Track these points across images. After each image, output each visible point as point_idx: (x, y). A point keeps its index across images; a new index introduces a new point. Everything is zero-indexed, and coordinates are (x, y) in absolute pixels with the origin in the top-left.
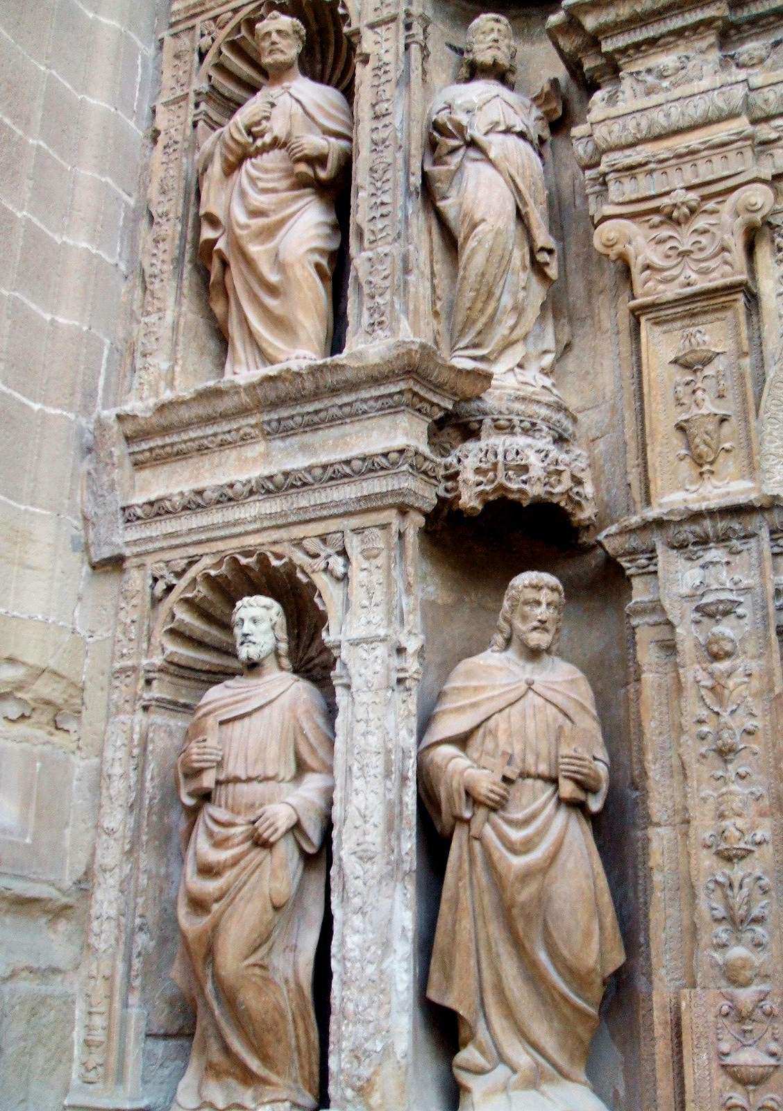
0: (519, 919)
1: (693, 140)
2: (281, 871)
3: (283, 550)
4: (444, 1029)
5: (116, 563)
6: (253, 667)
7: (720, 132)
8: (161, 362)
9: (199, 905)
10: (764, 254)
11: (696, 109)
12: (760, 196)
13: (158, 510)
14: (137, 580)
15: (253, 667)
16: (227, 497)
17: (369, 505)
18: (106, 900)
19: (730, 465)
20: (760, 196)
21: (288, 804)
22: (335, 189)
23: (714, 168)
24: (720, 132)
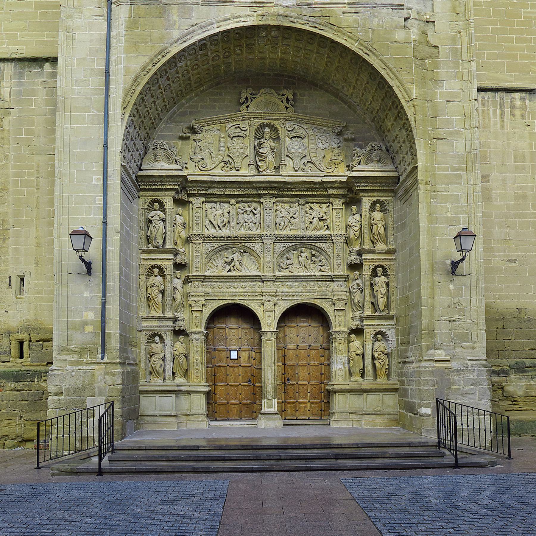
0: (180, 365)
2: (161, 362)
3: (159, 332)
4: (174, 373)
6: (157, 343)
8: (143, 309)
9: (154, 364)
12: (204, 302)
13: (146, 327)
14: (143, 333)
15: (157, 343)
16: (154, 327)
19: (199, 327)
20: (204, 302)
21: (162, 355)
22: (163, 292)
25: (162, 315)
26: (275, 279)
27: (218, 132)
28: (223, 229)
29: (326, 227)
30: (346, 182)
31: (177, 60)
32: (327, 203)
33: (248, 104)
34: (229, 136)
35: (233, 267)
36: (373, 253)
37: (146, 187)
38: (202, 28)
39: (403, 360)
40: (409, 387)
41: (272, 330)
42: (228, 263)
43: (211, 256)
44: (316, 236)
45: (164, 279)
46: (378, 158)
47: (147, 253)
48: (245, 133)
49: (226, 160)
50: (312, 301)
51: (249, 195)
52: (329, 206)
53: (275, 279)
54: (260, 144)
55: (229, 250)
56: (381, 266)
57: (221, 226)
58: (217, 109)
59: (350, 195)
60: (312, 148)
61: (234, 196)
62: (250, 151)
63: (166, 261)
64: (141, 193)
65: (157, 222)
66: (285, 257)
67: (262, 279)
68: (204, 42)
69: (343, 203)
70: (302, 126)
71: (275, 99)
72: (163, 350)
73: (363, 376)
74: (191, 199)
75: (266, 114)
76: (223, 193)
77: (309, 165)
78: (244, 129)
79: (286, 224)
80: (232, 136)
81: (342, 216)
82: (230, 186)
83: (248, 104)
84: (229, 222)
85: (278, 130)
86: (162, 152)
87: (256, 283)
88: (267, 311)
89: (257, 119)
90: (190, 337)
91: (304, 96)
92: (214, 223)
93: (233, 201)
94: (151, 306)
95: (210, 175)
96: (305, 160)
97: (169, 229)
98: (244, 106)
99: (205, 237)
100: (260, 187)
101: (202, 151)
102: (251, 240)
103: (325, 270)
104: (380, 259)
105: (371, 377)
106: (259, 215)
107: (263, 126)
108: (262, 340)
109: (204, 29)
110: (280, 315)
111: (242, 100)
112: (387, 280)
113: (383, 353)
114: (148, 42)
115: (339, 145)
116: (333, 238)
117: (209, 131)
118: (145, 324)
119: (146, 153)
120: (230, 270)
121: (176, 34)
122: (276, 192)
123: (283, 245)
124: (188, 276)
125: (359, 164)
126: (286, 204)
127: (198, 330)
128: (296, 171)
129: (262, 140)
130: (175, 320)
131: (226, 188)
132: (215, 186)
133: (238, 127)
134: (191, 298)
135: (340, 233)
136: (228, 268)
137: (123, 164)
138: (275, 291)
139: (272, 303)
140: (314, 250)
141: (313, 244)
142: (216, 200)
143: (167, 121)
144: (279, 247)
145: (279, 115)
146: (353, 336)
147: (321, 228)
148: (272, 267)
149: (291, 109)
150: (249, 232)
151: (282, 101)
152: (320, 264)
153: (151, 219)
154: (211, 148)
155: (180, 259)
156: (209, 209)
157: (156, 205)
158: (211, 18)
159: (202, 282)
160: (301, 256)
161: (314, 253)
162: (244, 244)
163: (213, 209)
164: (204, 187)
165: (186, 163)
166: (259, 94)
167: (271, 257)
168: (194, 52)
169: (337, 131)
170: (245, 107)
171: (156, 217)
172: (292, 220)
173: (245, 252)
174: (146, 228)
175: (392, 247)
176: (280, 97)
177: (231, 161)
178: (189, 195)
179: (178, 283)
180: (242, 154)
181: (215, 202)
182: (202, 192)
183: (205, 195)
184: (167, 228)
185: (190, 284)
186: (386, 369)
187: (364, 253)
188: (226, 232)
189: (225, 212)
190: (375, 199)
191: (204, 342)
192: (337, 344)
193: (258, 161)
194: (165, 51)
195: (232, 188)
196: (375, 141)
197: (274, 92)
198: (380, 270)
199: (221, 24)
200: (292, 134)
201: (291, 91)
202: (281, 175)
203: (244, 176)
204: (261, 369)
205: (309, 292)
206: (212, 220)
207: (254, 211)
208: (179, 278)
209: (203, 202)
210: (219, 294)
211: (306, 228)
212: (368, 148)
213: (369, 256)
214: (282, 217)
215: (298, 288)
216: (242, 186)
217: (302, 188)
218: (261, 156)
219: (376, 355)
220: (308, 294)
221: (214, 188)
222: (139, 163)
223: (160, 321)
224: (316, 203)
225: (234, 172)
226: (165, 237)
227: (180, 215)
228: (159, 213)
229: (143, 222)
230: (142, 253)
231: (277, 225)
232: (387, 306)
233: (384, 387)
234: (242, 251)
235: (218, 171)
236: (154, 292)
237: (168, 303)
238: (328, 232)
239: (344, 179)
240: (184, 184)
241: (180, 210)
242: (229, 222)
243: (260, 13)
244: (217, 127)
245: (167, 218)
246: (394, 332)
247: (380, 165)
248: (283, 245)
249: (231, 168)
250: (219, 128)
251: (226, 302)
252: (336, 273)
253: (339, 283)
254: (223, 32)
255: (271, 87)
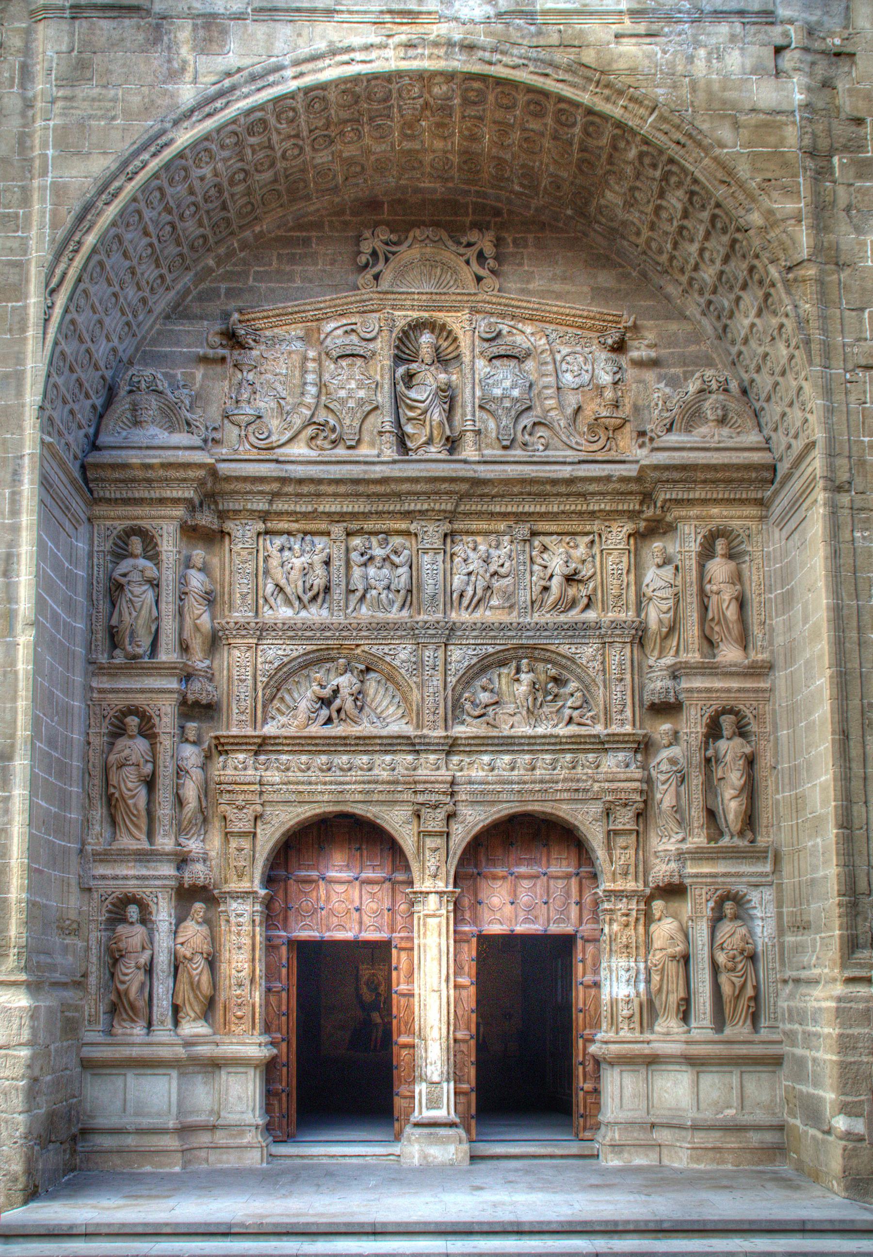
1: (246, 787)
3: (140, 893)
5: (90, 890)
6: (132, 923)
7: (252, 788)
8: (97, 828)
9: (123, 982)
10: (259, 823)
11: (248, 779)
12: (259, 808)
14: (95, 895)
15: (132, 923)
16: (126, 878)
17: (164, 887)
18: (93, 980)
19: (245, 879)
20: (259, 808)
21: (144, 958)
22: (150, 783)
23: (249, 797)
24: (252, 788)
25: (146, 846)
26: (451, 747)
27: (299, 344)
28: (313, 609)
29: (585, 601)
30: (639, 479)
31: (191, 162)
32: (587, 534)
33: (376, 270)
34: (327, 354)
35: (339, 711)
36: (711, 674)
37: (108, 495)
38: (253, 78)
39: (794, 974)
40: (806, 1053)
41: (441, 886)
42: (325, 702)
43: (280, 682)
44: (559, 627)
45: (153, 746)
46: (720, 412)
47: (110, 675)
48: (371, 346)
49: (320, 419)
50: (548, 808)
51: (379, 514)
52: (592, 542)
53: (451, 747)
54: (409, 377)
55: (328, 665)
56: (731, 711)
57: (306, 598)
58: (298, 283)
59: (649, 513)
60: (545, 387)
61: (341, 517)
62: (384, 398)
63: (160, 695)
64: (99, 510)
65: (137, 590)
66: (478, 683)
67: (413, 745)
68: (259, 114)
69: (630, 536)
70: (520, 326)
71: (449, 255)
72: (150, 941)
73: (685, 1017)
74: (229, 526)
75: (424, 297)
76: (310, 509)
77: (541, 431)
78: (368, 336)
79: (479, 593)
80: (335, 354)
81: (628, 571)
82: (331, 489)
83: (376, 270)
84: (327, 589)
85: (455, 339)
86: (154, 402)
87: (399, 757)
88: (430, 834)
89: (402, 308)
90: (222, 908)
91: (526, 246)
92: (288, 590)
93: (337, 530)
94: (119, 819)
95: (277, 461)
96: (526, 420)
97: (168, 608)
98: (369, 275)
99: (262, 631)
100: (408, 493)
101: (258, 396)
102: (384, 638)
103: (583, 721)
104: (729, 690)
105: (707, 1022)
106: (405, 569)
107: (418, 326)
108: (416, 916)
109: (260, 83)
110: (464, 844)
111: (363, 259)
112: (748, 750)
113: (741, 953)
114: (114, 118)
115: (618, 376)
116: (603, 631)
117: (275, 341)
118: (102, 870)
119: (109, 401)
120: (329, 721)
121: (187, 94)
122: (449, 507)
123: (470, 652)
124: (217, 738)
125: (669, 430)
126: (479, 539)
127: (244, 885)
128: (505, 448)
129: (414, 366)
130: (182, 860)
131: (319, 495)
132: (289, 489)
133: (353, 330)
134: (226, 796)
135: (623, 616)
136: (324, 713)
137: (48, 439)
138: (449, 779)
139: (441, 814)
140: (554, 663)
141: (553, 648)
142: (295, 526)
143: (168, 317)
144: (460, 657)
145: (459, 298)
146: (658, 905)
147: (573, 603)
148: (441, 710)
149: (490, 281)
150: (380, 615)
151: (468, 262)
152: (569, 704)
153: (123, 580)
154: (280, 388)
155: (198, 690)
156: (275, 553)
157: (136, 545)
158: (276, 52)
159: (257, 753)
160: (518, 680)
161: (553, 672)
162: (366, 648)
163: (287, 553)
164: (261, 492)
165: (215, 429)
166: (406, 244)
167: (441, 684)
168: (234, 140)
169: (610, 341)
170: (369, 277)
171: (135, 576)
172: (497, 584)
173: (368, 669)
174: (108, 606)
175: (760, 657)
176: (462, 250)
177: (332, 422)
178: (223, 515)
179: (191, 754)
180: (361, 402)
181: (289, 533)
182: (255, 507)
183: (264, 516)
184: (163, 606)
185: (222, 759)
186: (750, 998)
187: (687, 675)
188: (317, 614)
189: (317, 559)
190: (712, 525)
191: (258, 919)
192: (615, 927)
193: (403, 421)
194: (159, 142)
195: (335, 495)
196: (710, 364)
197: (445, 236)
198: (727, 722)
199: (304, 68)
200: (495, 349)
201: (490, 235)
202: (465, 462)
203: (366, 463)
204: (413, 995)
205: (541, 782)
206: (283, 582)
207: (393, 557)
208: (194, 743)
209: (259, 534)
210: (301, 788)
211: (533, 603)
212: (693, 387)
213: (698, 683)
214: (469, 574)
215: (513, 769)
216: (361, 489)
217: (521, 494)
218: (411, 408)
219: (721, 958)
220: (538, 787)
221: (286, 494)
222: (91, 431)
223: (140, 861)
224: (558, 534)
225: (341, 452)
226: (157, 630)
227: (200, 570)
228: (142, 562)
229: (100, 588)
230: (94, 674)
231: (453, 599)
232: (750, 821)
233: (743, 1050)
234: (363, 667)
235: (299, 450)
236: (129, 783)
237: (165, 810)
238: (591, 615)
239: (631, 471)
240: (209, 485)
241: (199, 554)
242: (327, 589)
243: (403, 38)
244: (297, 331)
245: (164, 577)
246: (768, 894)
247: (725, 431)
248: (470, 652)
249: (333, 442)
250: (301, 333)
251: (318, 810)
252: (615, 729)
253: (621, 756)
254: (307, 90)
255: (436, 224)
